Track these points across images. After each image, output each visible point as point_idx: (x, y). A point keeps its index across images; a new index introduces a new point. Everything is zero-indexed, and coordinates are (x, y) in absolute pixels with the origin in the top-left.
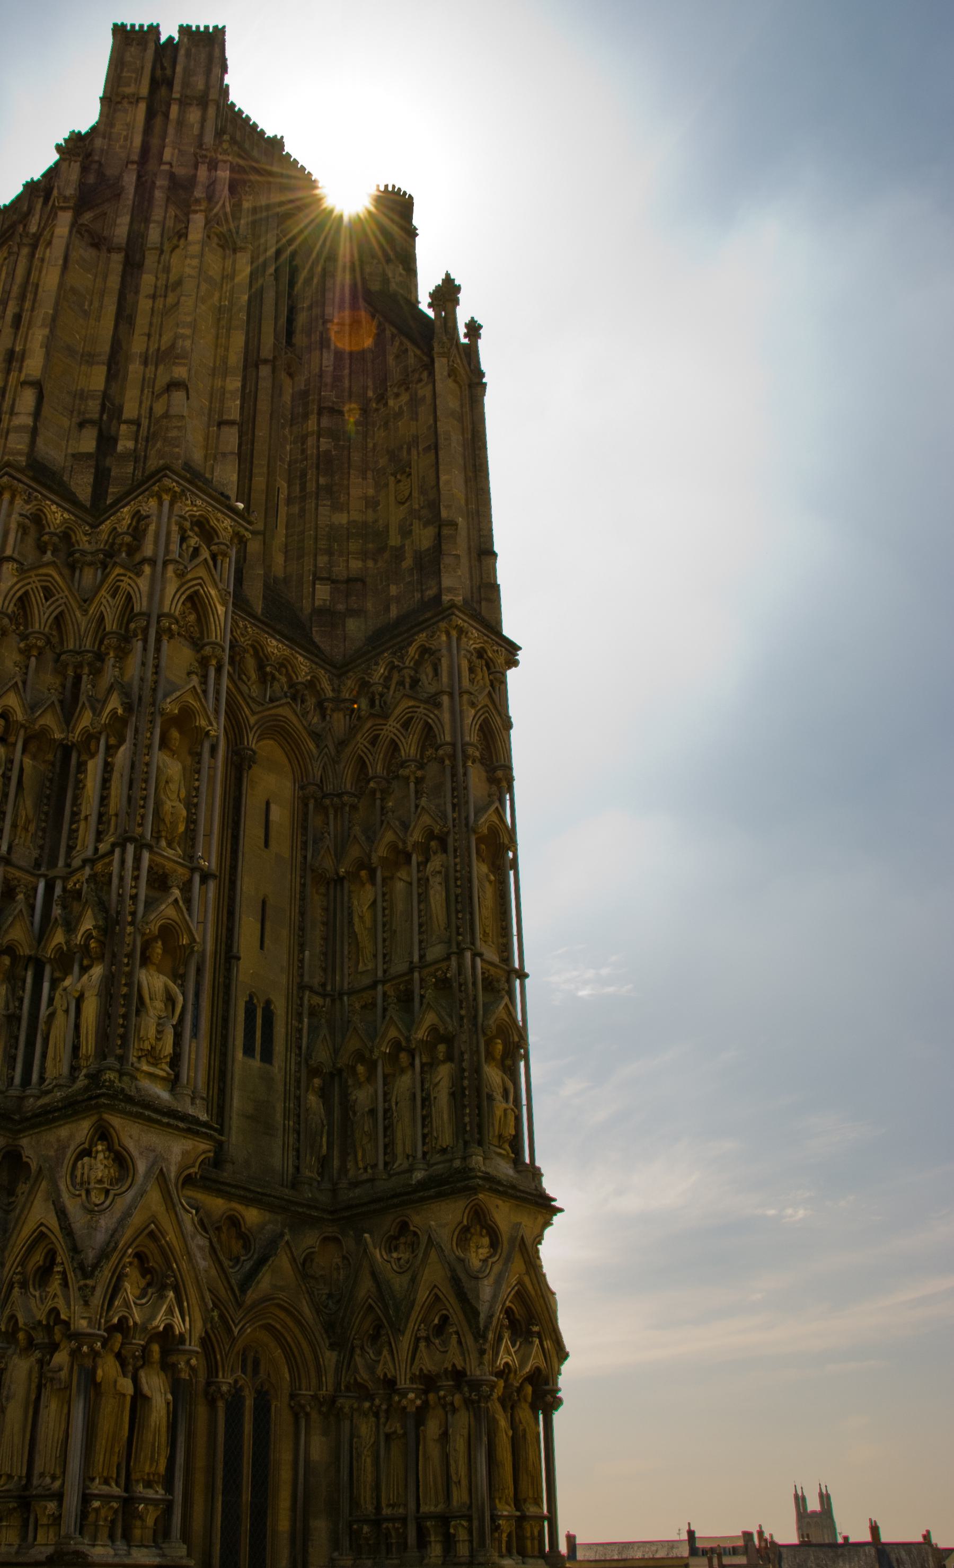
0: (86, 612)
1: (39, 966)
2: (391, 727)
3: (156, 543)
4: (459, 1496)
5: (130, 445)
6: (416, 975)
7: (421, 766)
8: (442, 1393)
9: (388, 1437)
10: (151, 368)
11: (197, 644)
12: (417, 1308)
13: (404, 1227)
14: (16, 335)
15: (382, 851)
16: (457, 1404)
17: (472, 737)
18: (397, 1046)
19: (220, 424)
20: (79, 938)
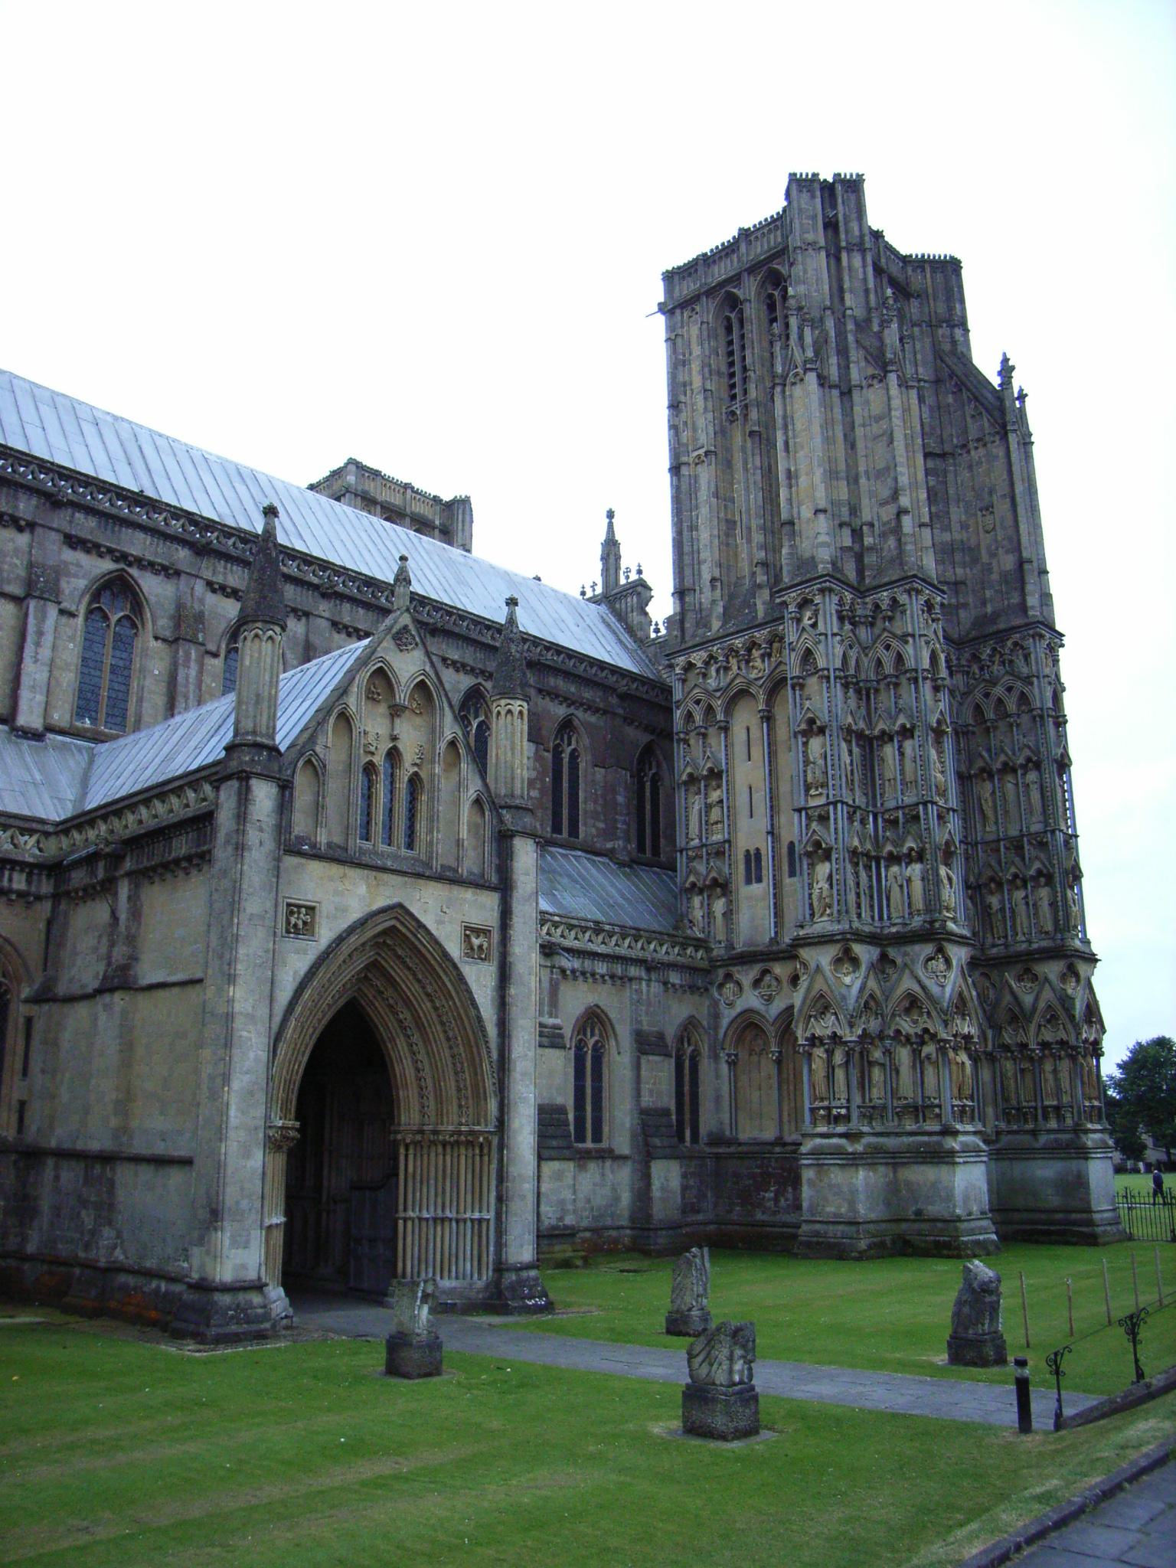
0: (866, 655)
1: (878, 859)
2: (998, 691)
3: (913, 624)
4: (1066, 1099)
5: (871, 540)
6: (1025, 839)
7: (1019, 716)
9: (1022, 1071)
10: (872, 481)
11: (934, 680)
12: (1038, 1011)
13: (1028, 970)
14: (789, 457)
15: (998, 765)
17: (1050, 705)
18: (1016, 876)
19: (920, 526)
20: (905, 850)
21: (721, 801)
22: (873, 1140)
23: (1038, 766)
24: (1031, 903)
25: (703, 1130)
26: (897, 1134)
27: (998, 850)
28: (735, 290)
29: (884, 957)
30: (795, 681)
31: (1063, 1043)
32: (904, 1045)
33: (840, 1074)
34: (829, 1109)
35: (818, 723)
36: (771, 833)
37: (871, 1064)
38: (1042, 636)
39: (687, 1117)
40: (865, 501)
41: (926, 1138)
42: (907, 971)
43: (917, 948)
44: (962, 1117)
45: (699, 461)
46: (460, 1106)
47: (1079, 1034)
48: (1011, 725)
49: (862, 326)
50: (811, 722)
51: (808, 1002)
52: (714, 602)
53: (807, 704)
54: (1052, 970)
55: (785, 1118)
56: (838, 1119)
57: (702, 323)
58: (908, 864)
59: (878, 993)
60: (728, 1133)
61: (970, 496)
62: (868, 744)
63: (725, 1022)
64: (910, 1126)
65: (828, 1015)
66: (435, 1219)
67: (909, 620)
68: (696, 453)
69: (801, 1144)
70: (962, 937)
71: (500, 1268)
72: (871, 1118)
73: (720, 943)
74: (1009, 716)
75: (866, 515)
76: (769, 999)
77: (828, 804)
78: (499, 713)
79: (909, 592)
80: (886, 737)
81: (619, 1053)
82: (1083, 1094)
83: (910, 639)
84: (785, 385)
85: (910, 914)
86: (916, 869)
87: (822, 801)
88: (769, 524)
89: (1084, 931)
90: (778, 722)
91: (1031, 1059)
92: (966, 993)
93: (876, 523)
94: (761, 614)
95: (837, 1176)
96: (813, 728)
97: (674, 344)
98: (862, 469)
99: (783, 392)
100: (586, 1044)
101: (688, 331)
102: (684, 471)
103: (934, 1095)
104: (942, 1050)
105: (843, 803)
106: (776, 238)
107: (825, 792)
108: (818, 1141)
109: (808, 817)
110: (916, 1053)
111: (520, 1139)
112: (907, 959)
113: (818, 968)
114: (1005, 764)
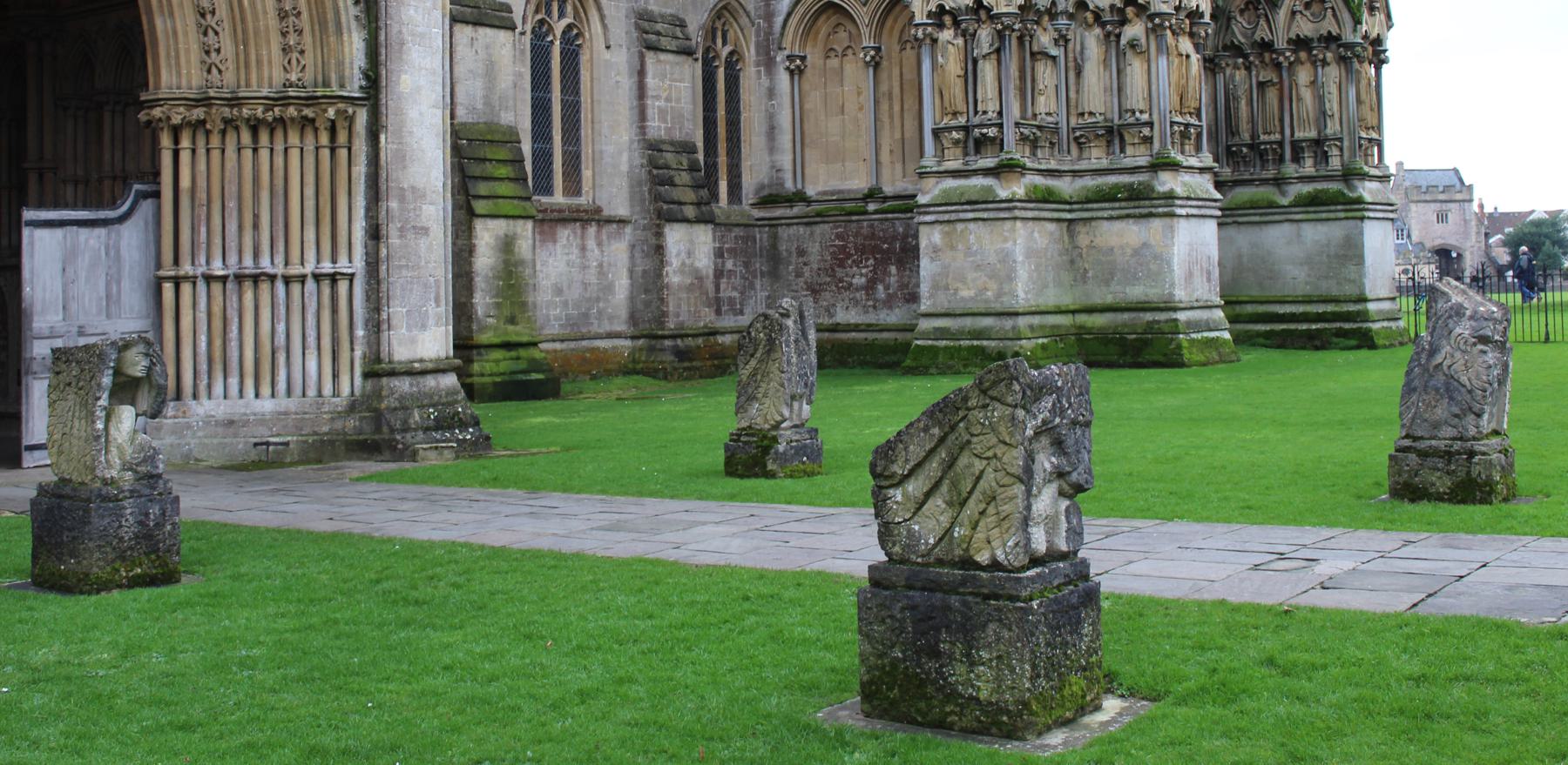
4: (1332, 128)
8: (1315, 52)
16: (1328, 60)
22: (1039, 180)
25: (749, 182)
26: (1076, 173)
31: (1330, 39)
33: (987, 70)
34: (966, 129)
39: (722, 159)
41: (1126, 179)
44: (1182, 144)
46: (286, 50)
47: (1357, 22)
55: (885, 157)
56: (981, 144)
60: (789, 185)
64: (1097, 156)
66: (240, 278)
71: (377, 369)
72: (1034, 144)
81: (608, 47)
91: (1278, 66)
95: (981, 238)
100: (550, 29)
103: (1142, 106)
104: (1155, 31)
108: (950, 183)
110: (1111, 39)
111: (412, 113)
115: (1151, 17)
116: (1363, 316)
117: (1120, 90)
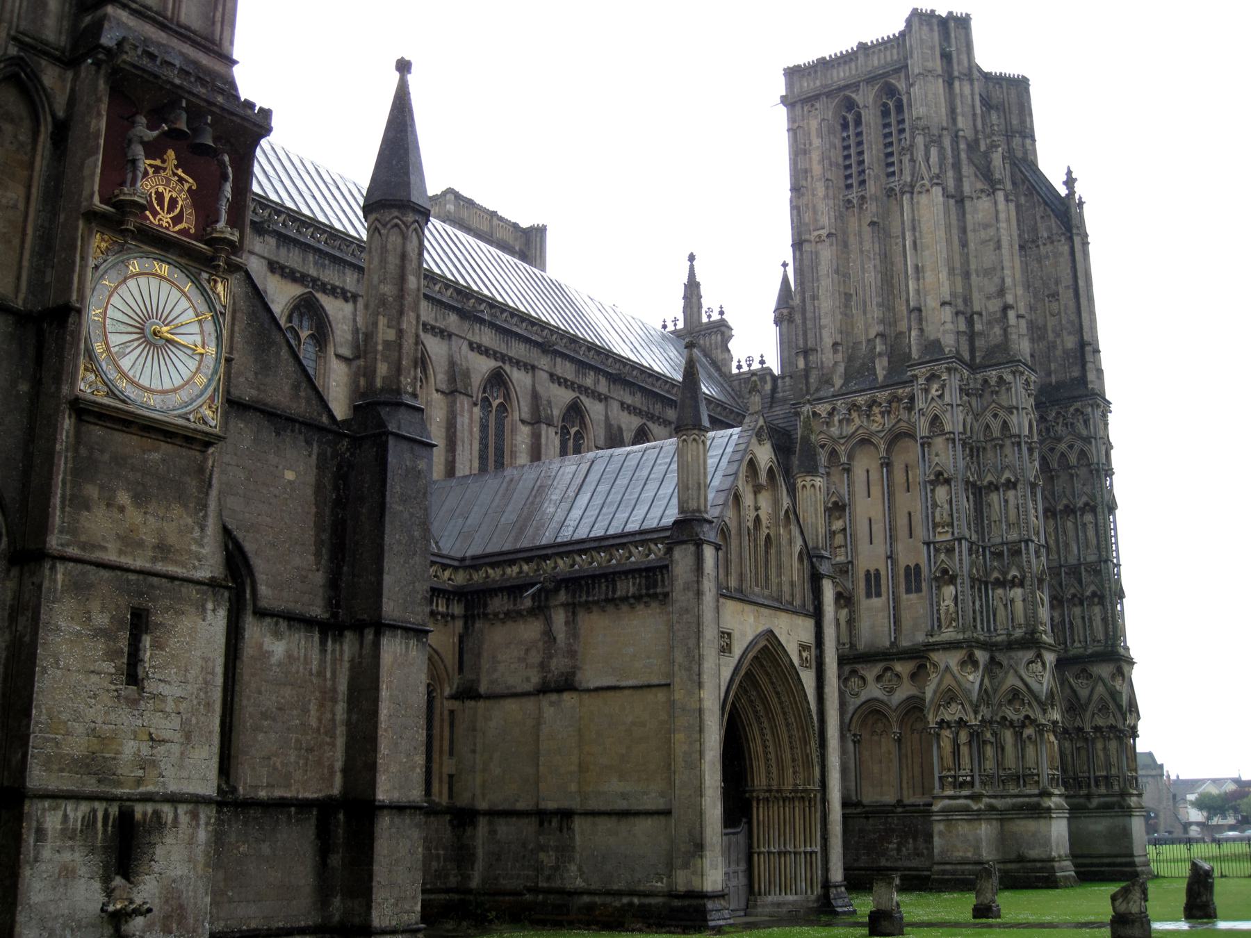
1: (986, 584)
3: (1017, 400)
4: (1114, 771)
6: (1083, 567)
9: (1078, 749)
13: (1084, 670)
18: (1074, 596)
20: (1009, 577)
21: (844, 530)
23: (1094, 510)
24: (1087, 617)
26: (1002, 797)
27: (1059, 574)
28: (854, 96)
29: (992, 659)
30: (925, 440)
31: (1112, 727)
32: (1008, 728)
33: (964, 750)
34: (954, 777)
35: (946, 475)
36: (890, 557)
37: (985, 742)
38: (1098, 406)
40: (976, 296)
41: (1027, 800)
42: (1012, 671)
43: (1020, 654)
45: (819, 240)
48: (1072, 476)
49: (973, 146)
50: (940, 474)
51: (938, 694)
52: (836, 363)
53: (936, 460)
54: (1104, 670)
55: (905, 785)
56: (962, 785)
57: (823, 120)
58: (1011, 588)
59: (990, 690)
60: (854, 798)
61: (1038, 284)
62: (978, 492)
63: (851, 709)
65: (954, 705)
67: (1014, 395)
68: (816, 233)
69: (931, 805)
70: (1050, 645)
73: (844, 644)
74: (1070, 468)
75: (977, 308)
76: (891, 691)
77: (955, 540)
78: (804, 486)
79: (1014, 373)
80: (993, 487)
82: (1128, 766)
83: (1015, 411)
84: (912, 193)
85: (1013, 626)
86: (1017, 593)
87: (949, 537)
88: (886, 302)
89: (1125, 641)
90: (895, 467)
91: (1086, 740)
92: (1054, 689)
93: (984, 313)
94: (880, 378)
95: (963, 828)
96: (940, 478)
97: (795, 134)
98: (973, 267)
99: (912, 199)
101: (808, 124)
102: (806, 247)
105: (966, 539)
106: (894, 55)
107: (950, 530)
108: (947, 802)
109: (937, 550)
110: (1018, 735)
112: (1012, 662)
113: (947, 668)
114: (1067, 506)
115: (1038, 726)
116: (1133, 864)
117: (1023, 757)
